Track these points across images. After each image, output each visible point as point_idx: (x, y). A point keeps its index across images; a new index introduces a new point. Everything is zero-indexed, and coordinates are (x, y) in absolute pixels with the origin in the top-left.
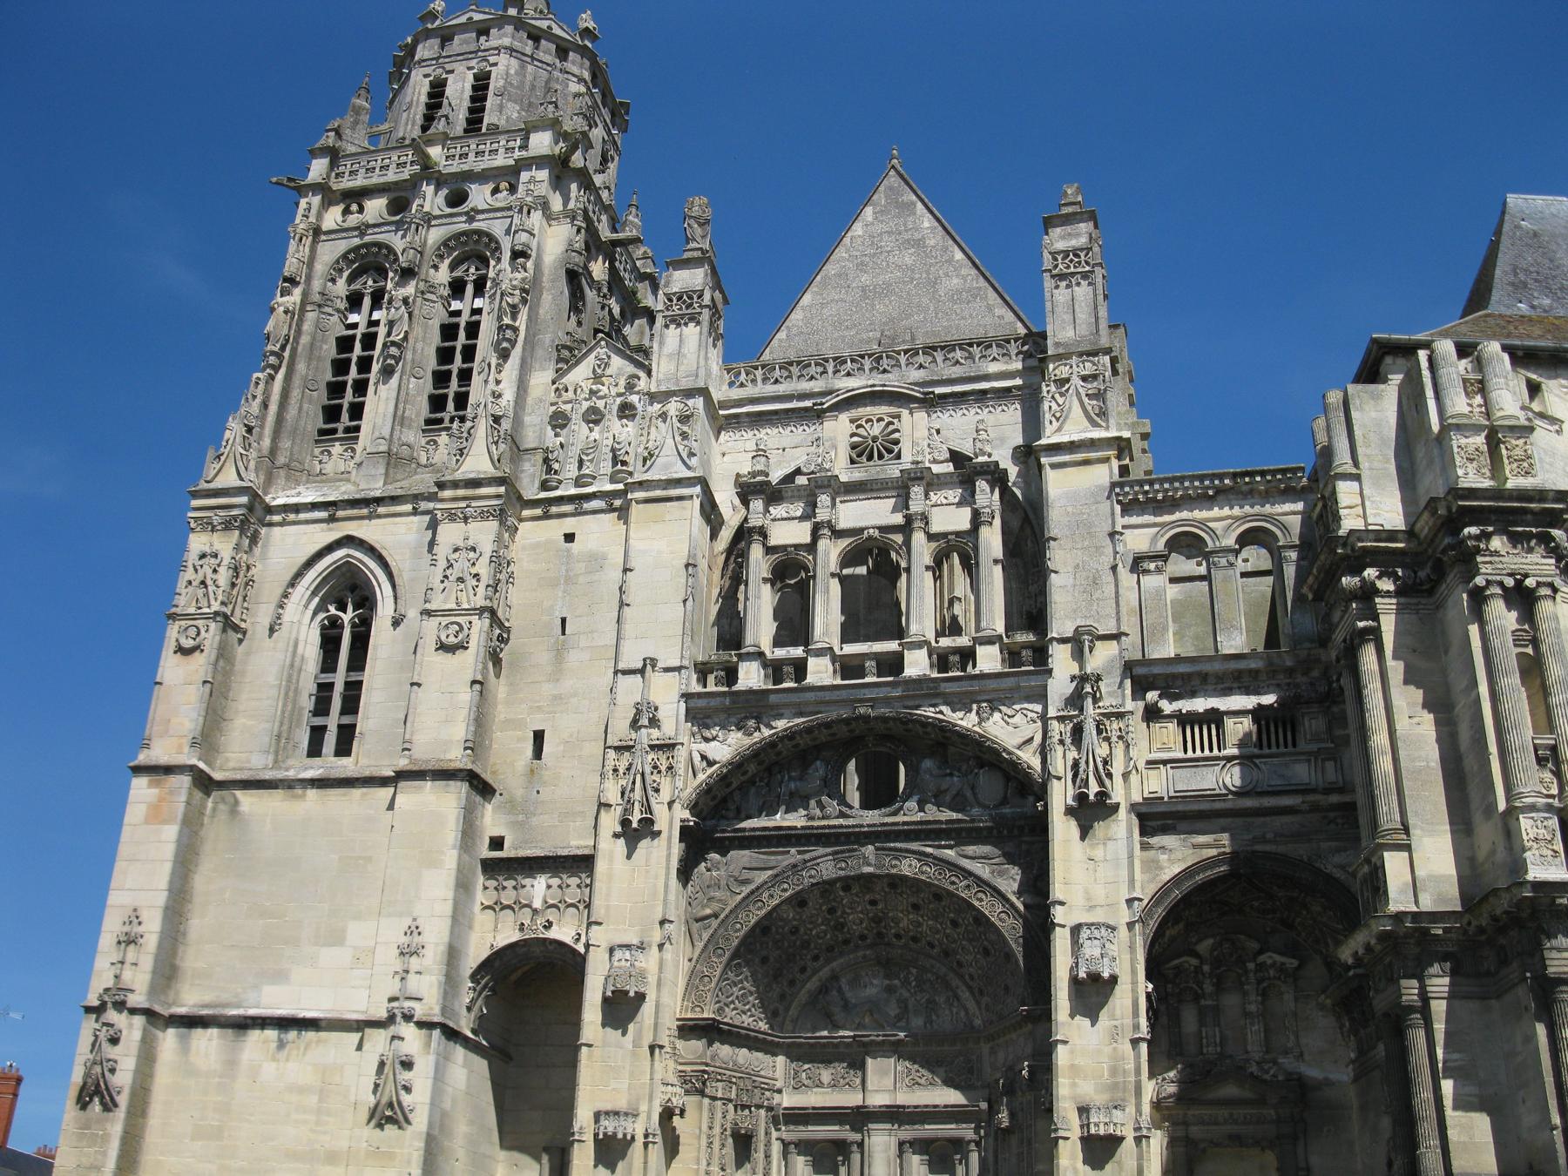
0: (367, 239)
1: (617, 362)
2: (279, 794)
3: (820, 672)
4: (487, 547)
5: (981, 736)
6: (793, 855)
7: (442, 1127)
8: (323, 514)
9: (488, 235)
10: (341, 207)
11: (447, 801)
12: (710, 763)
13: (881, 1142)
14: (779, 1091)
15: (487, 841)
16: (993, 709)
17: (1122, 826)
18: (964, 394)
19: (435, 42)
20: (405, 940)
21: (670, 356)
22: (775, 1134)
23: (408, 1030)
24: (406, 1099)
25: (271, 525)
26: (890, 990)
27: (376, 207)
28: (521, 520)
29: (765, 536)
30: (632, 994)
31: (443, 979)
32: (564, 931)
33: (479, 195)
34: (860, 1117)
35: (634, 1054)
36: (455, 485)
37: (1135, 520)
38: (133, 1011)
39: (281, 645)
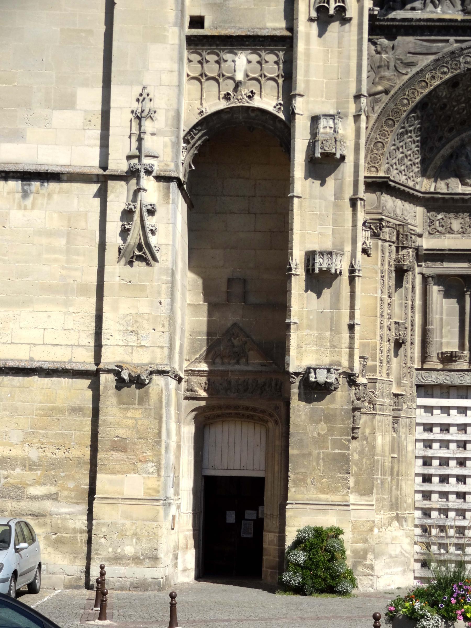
6: (452, 43)
14: (420, 236)
20: (136, 106)
22: (417, 270)
23: (148, 182)
32: (268, 101)
35: (336, 206)
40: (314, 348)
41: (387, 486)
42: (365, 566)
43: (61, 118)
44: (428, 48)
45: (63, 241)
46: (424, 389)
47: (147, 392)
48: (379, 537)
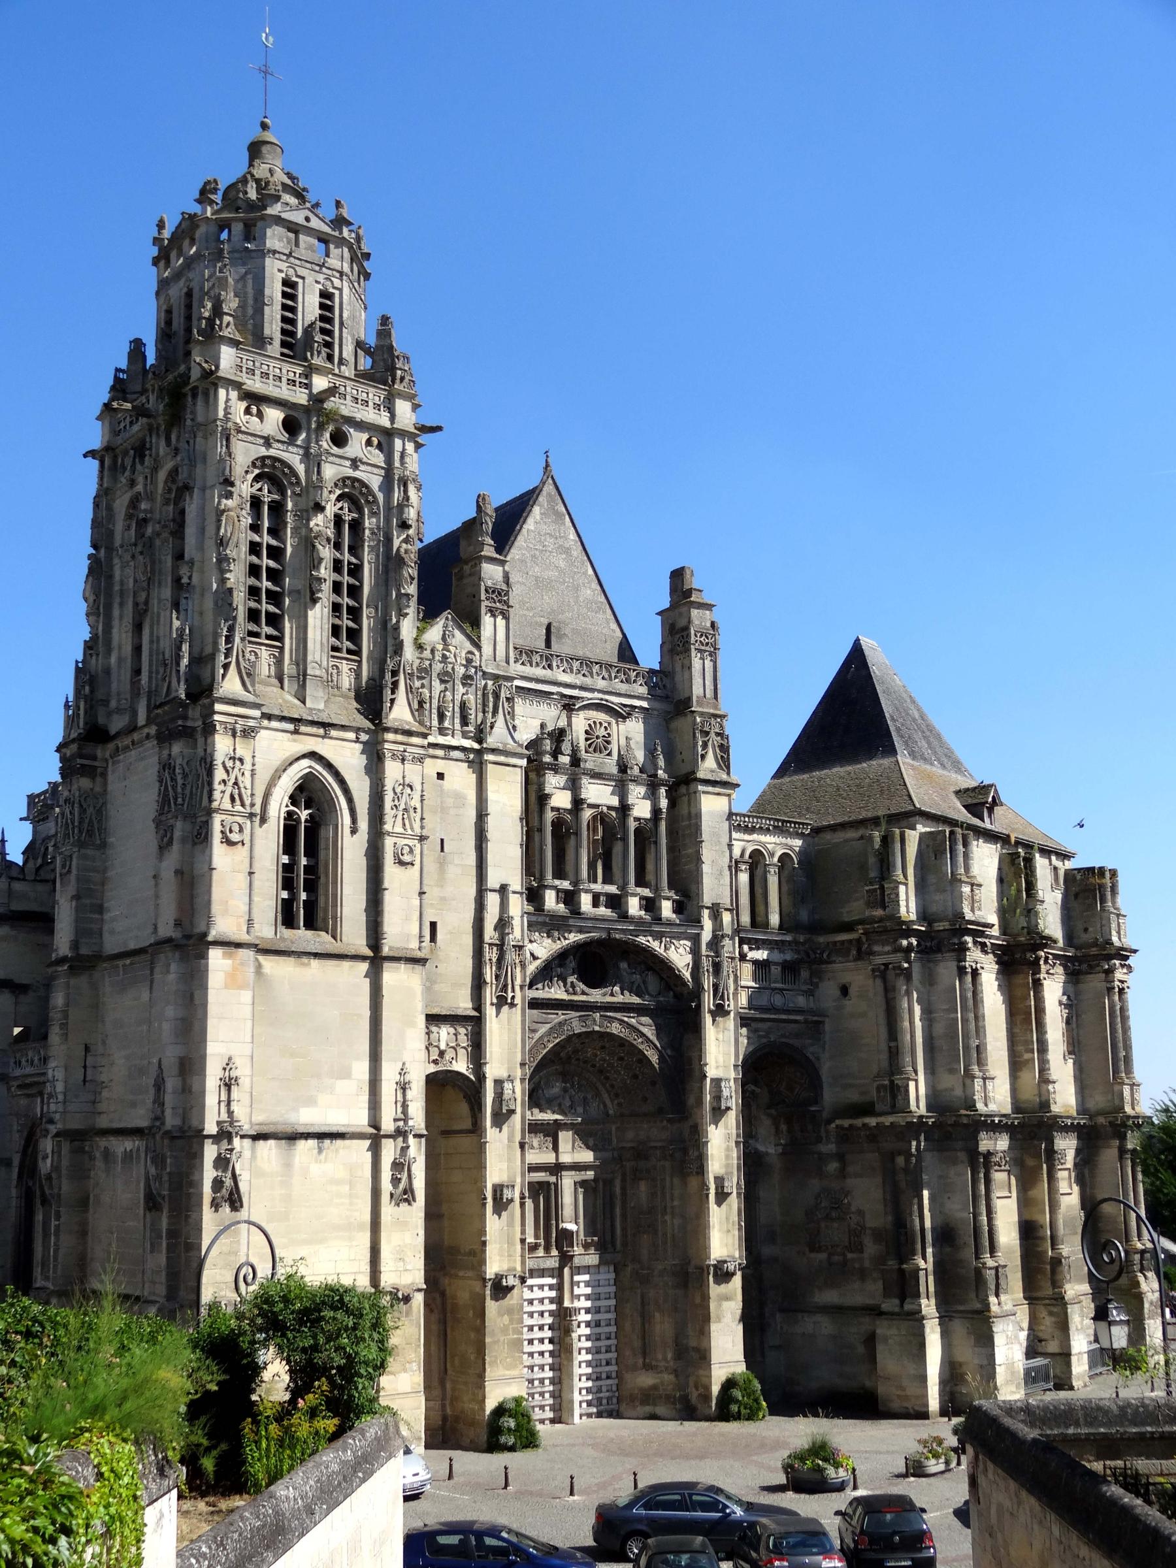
0: (272, 452)
2: (292, 960)
8: (291, 727)
9: (367, 487)
10: (244, 405)
12: (535, 958)
21: (488, 639)
26: (565, 1090)
32: (461, 1066)
33: (357, 442)
34: (557, 1169)
35: (509, 1147)
43: (342, 1086)
45: (347, 1188)
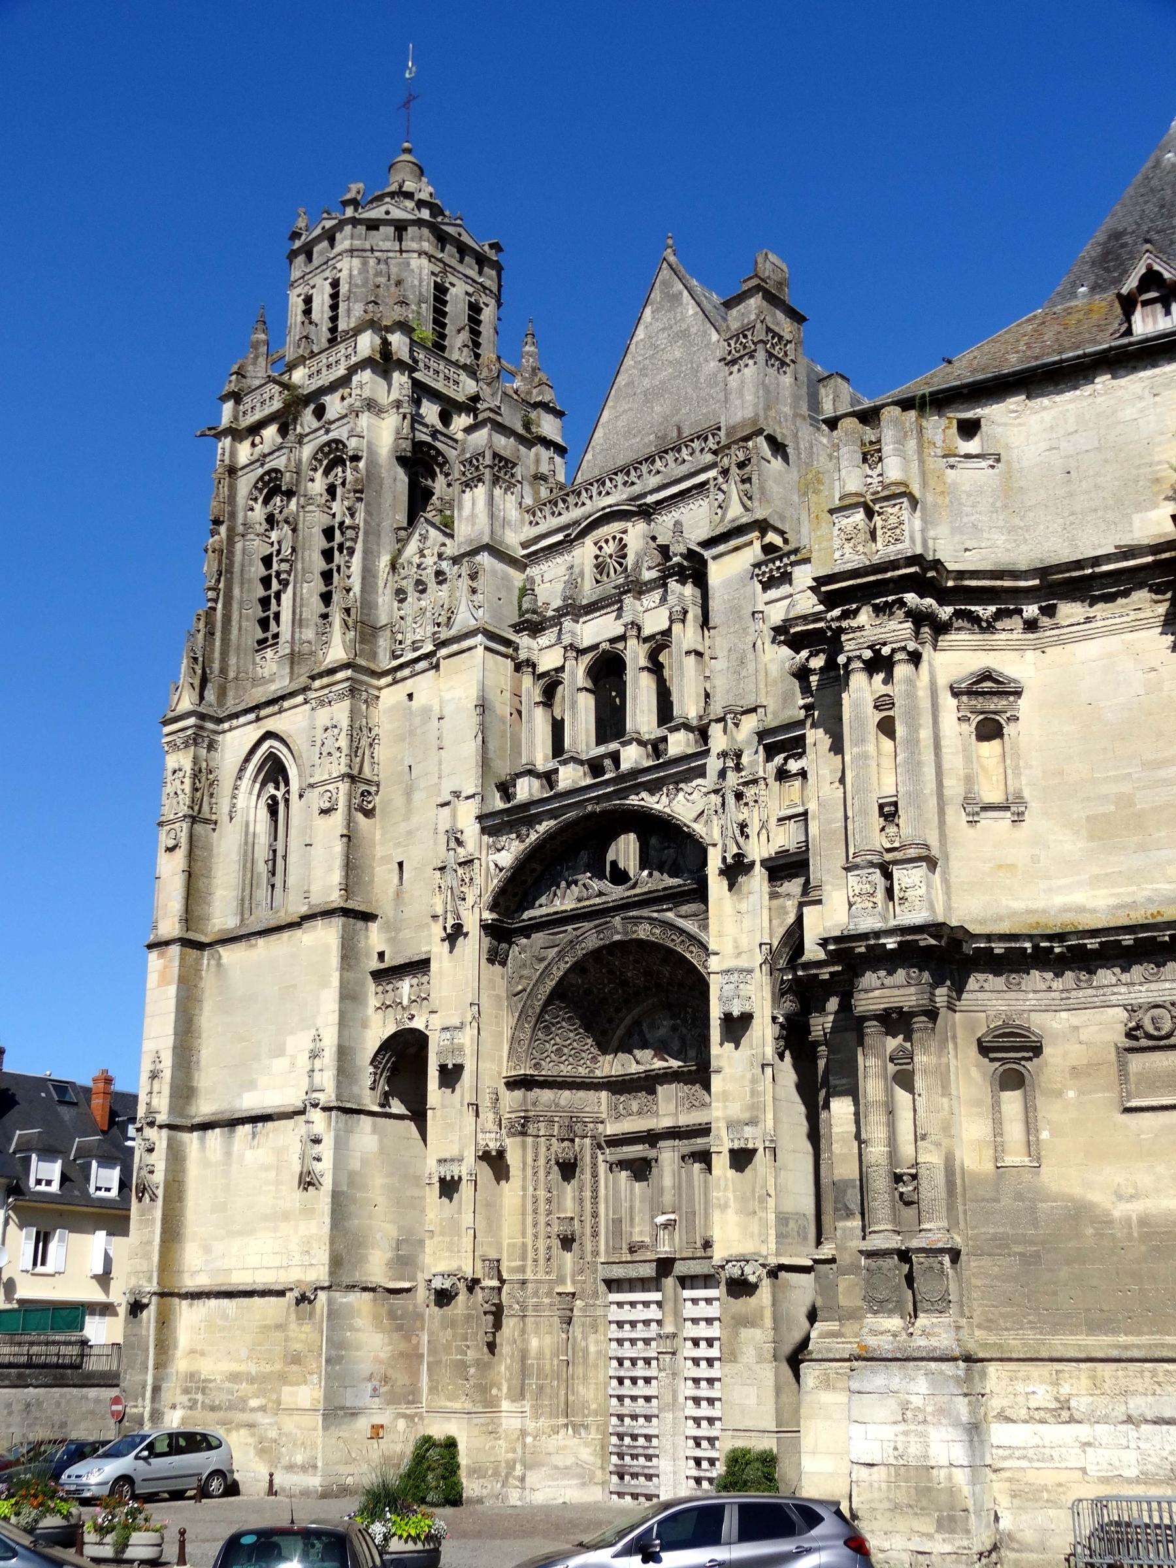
0: (267, 467)
1: (433, 533)
3: (570, 776)
4: (345, 723)
5: (669, 815)
7: (351, 1184)
8: (252, 716)
9: (341, 442)
11: (325, 937)
13: (668, 1155)
15: (376, 956)
16: (678, 790)
17: (758, 879)
18: (689, 490)
19: (301, 259)
23: (316, 1115)
24: (318, 1167)
25: (224, 732)
26: (674, 1029)
27: (270, 433)
28: (380, 689)
29: (534, 666)
30: (450, 1066)
31: (335, 1072)
34: (652, 1138)
36: (321, 675)
37: (773, 593)
38: (161, 1127)
39: (238, 828)
40: (447, 1254)
41: (548, 1390)
42: (514, 1478)
44: (553, 941)
46: (613, 1284)
47: (314, 1307)
48: (534, 1446)
